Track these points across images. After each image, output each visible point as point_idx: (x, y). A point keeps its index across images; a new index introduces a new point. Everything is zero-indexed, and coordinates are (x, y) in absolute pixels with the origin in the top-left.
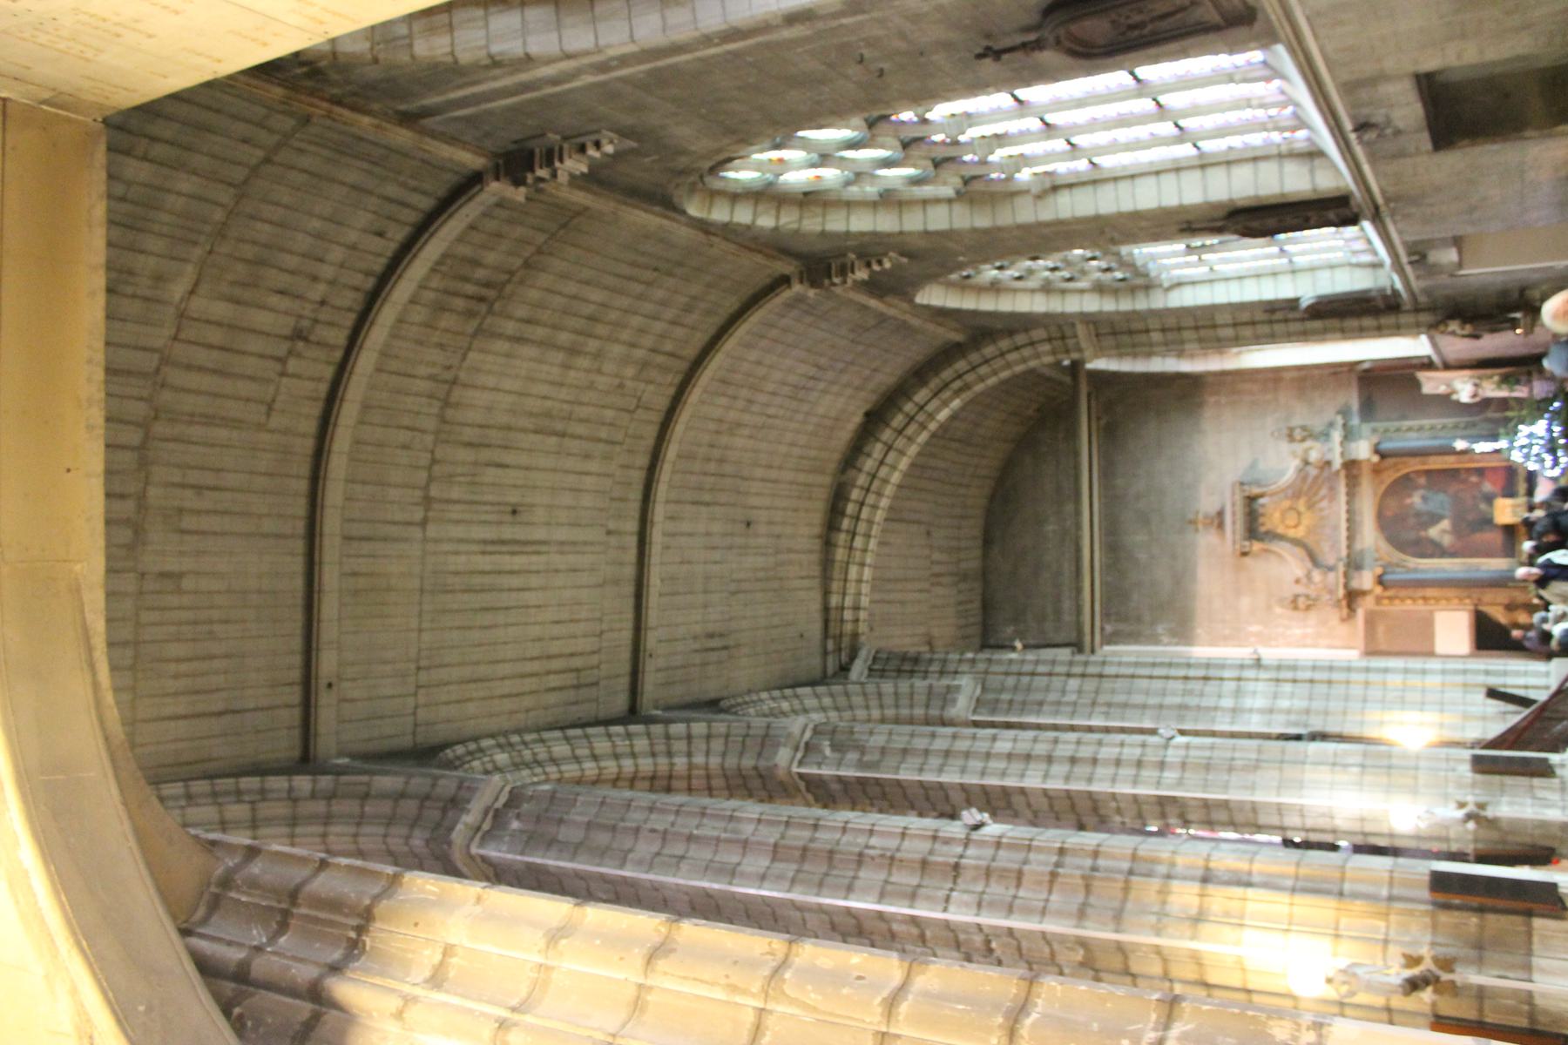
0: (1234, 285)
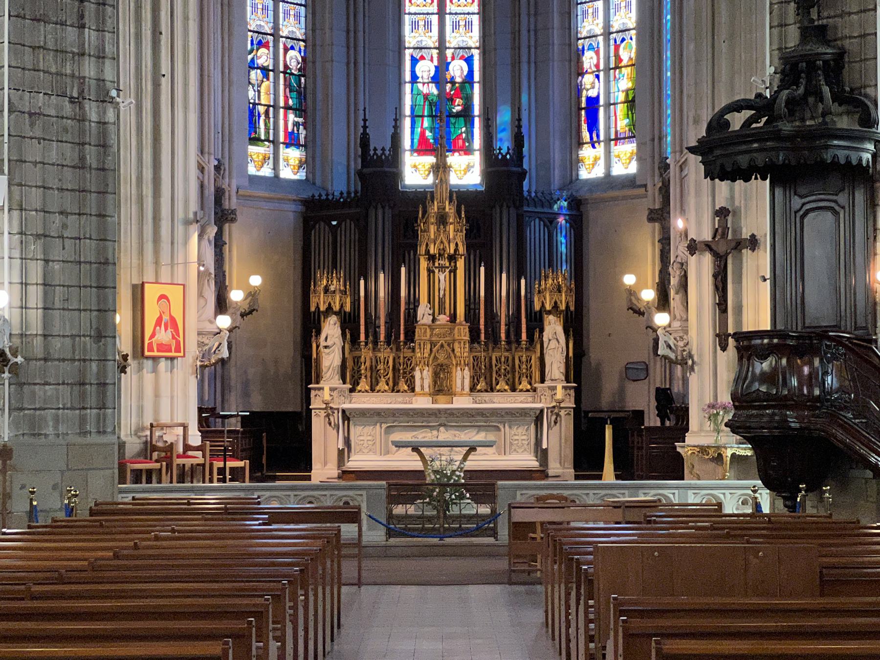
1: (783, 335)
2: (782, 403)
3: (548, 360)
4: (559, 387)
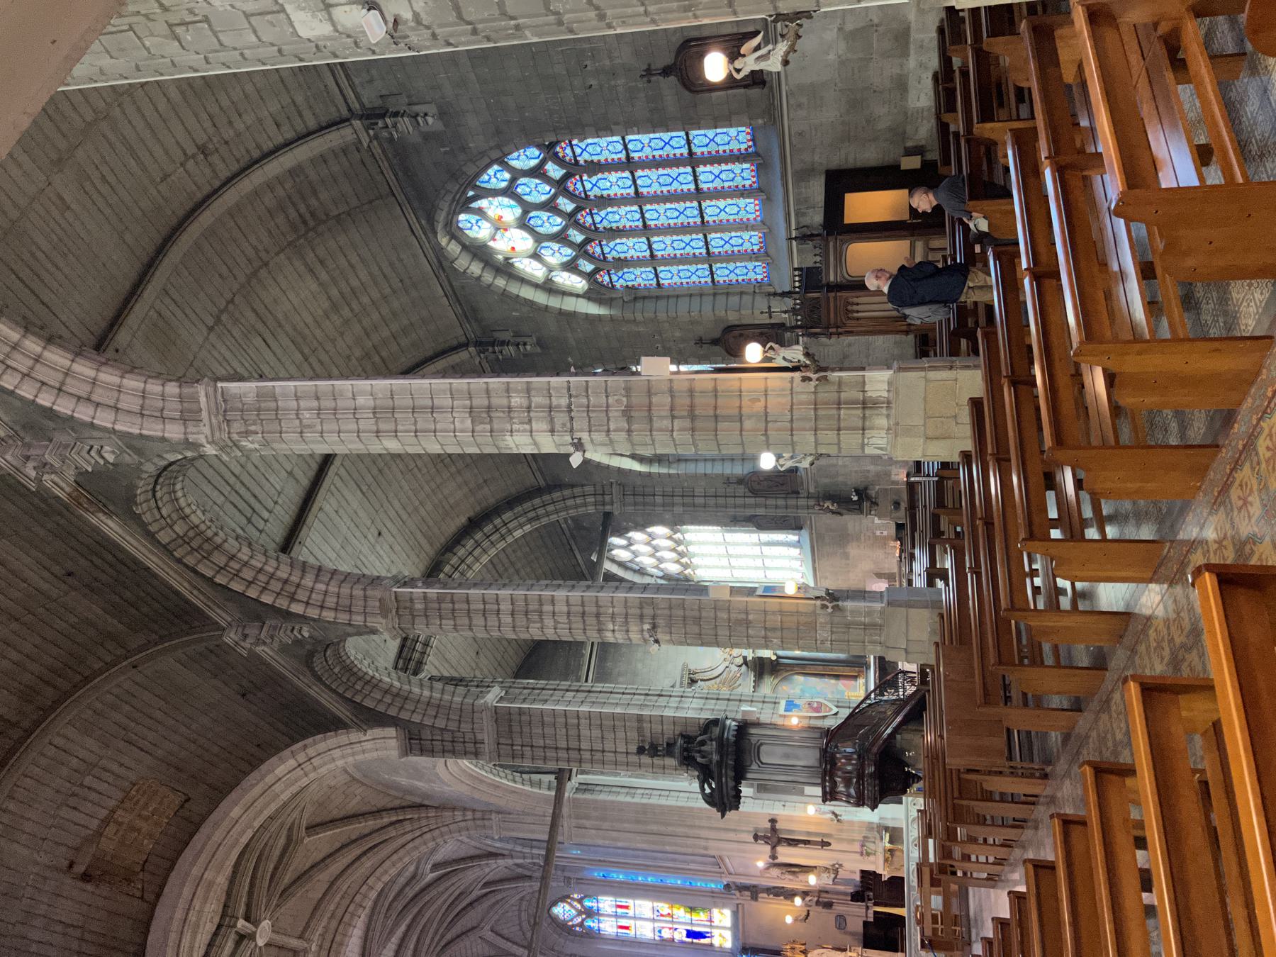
0: (709, 465)
1: (825, 773)
2: (860, 776)
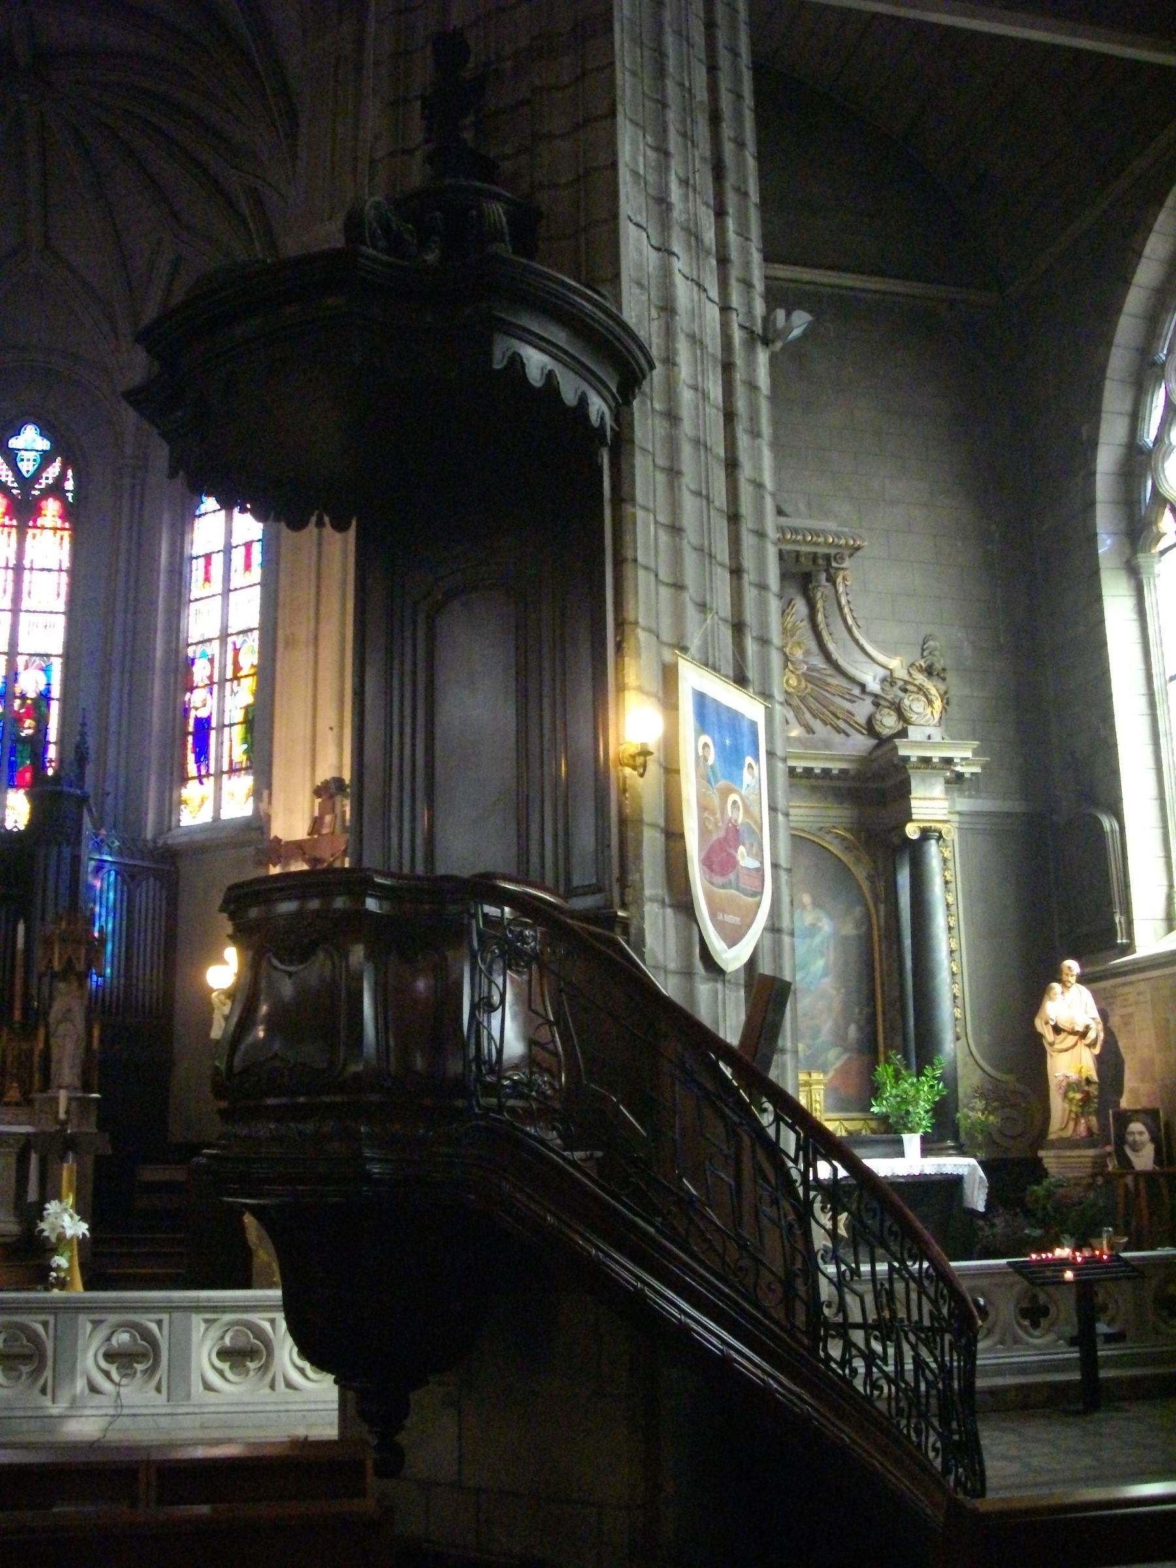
3: (55, 1053)
4: (63, 1095)
